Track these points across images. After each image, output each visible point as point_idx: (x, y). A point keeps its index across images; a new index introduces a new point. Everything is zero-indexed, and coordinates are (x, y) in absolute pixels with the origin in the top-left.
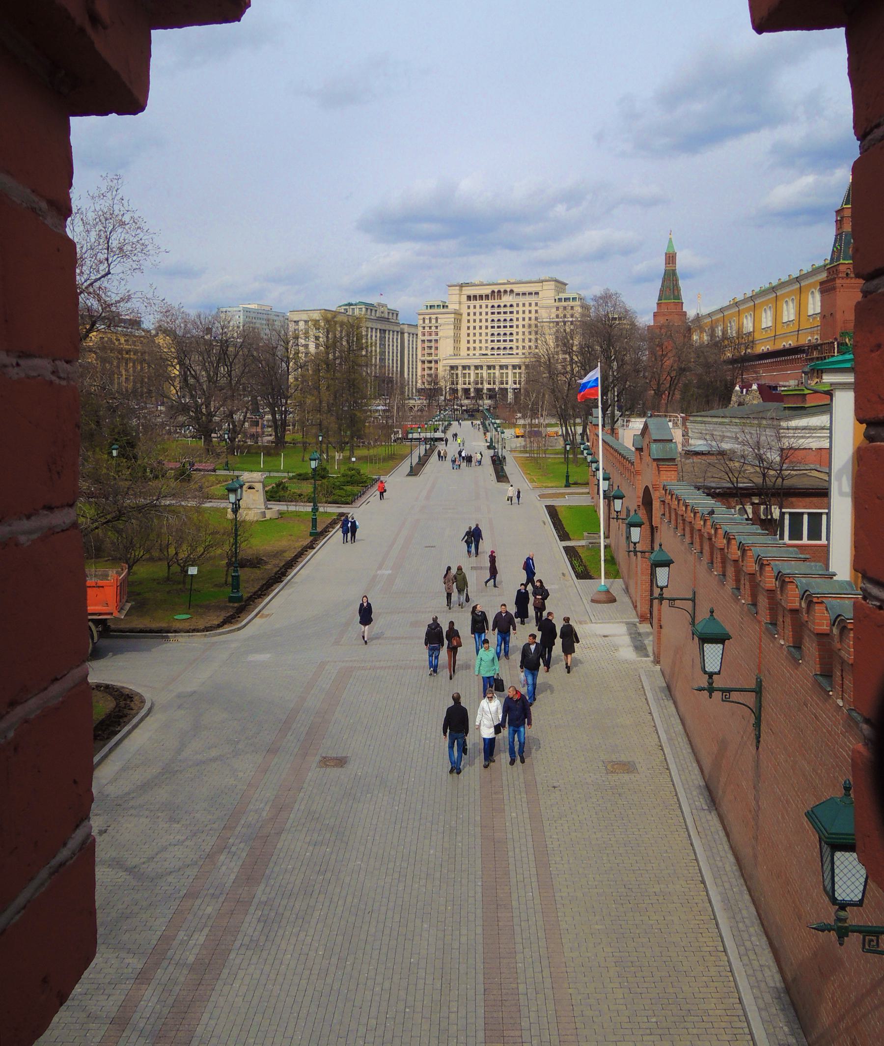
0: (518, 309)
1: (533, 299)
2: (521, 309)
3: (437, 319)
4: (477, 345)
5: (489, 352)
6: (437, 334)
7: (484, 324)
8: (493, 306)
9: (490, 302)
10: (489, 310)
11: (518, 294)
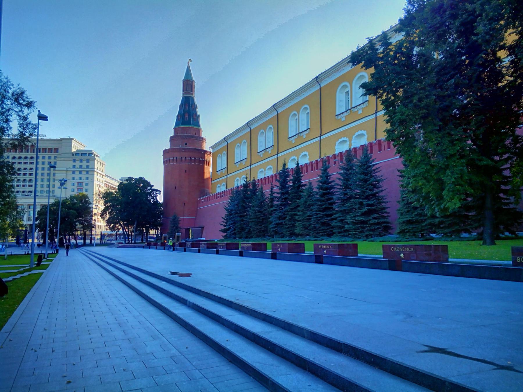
1: (53, 155)
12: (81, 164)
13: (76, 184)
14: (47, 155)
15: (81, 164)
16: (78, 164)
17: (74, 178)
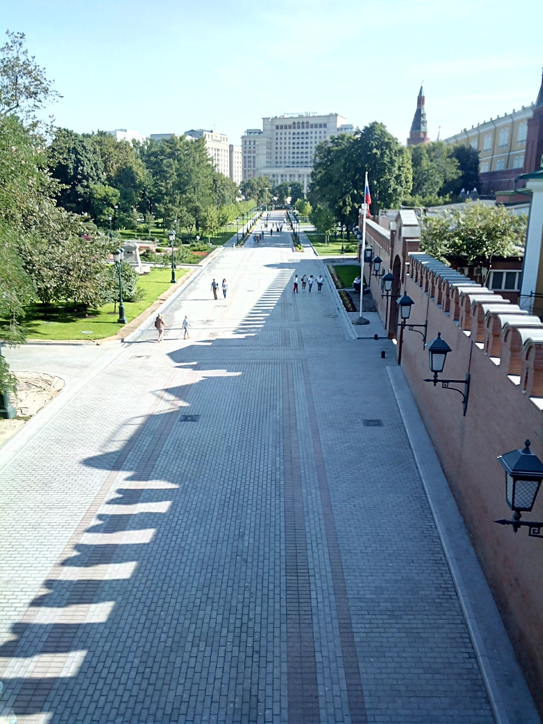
2: (314, 135)
3: (254, 142)
4: (283, 160)
5: (291, 165)
6: (254, 152)
8: (294, 134)
9: (292, 131)
10: (292, 136)
14: (318, 130)
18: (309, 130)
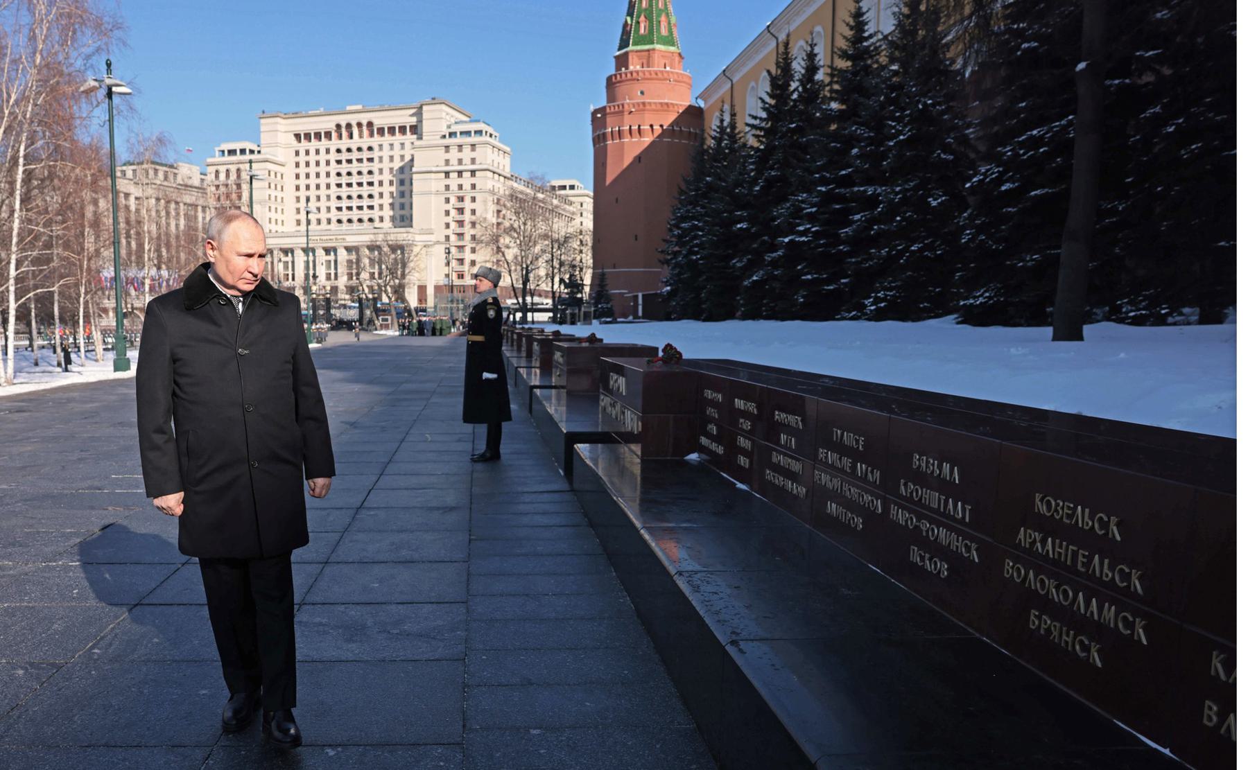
0: (381, 154)
2: (386, 153)
7: (323, 181)
9: (334, 143)
10: (333, 157)
11: (381, 131)
12: (460, 155)
13: (453, 200)
15: (460, 155)
16: (454, 155)
17: (447, 187)
18: (376, 140)
